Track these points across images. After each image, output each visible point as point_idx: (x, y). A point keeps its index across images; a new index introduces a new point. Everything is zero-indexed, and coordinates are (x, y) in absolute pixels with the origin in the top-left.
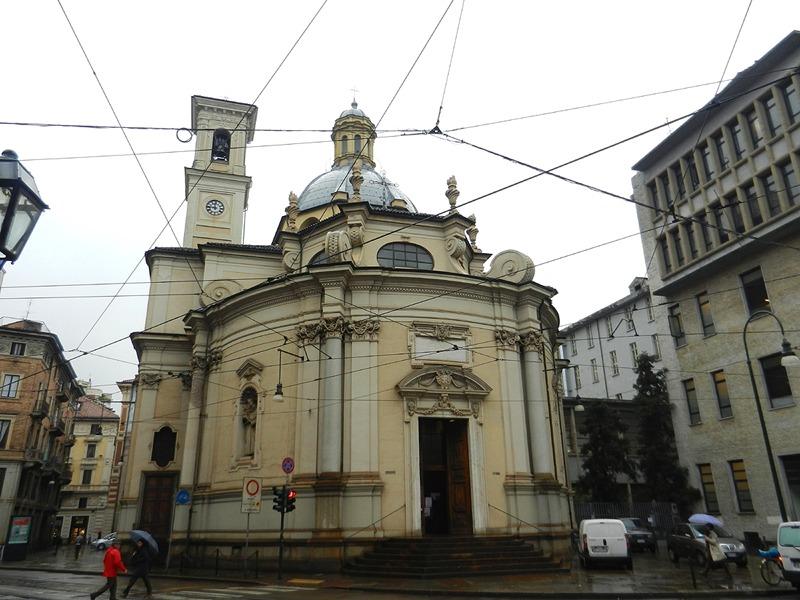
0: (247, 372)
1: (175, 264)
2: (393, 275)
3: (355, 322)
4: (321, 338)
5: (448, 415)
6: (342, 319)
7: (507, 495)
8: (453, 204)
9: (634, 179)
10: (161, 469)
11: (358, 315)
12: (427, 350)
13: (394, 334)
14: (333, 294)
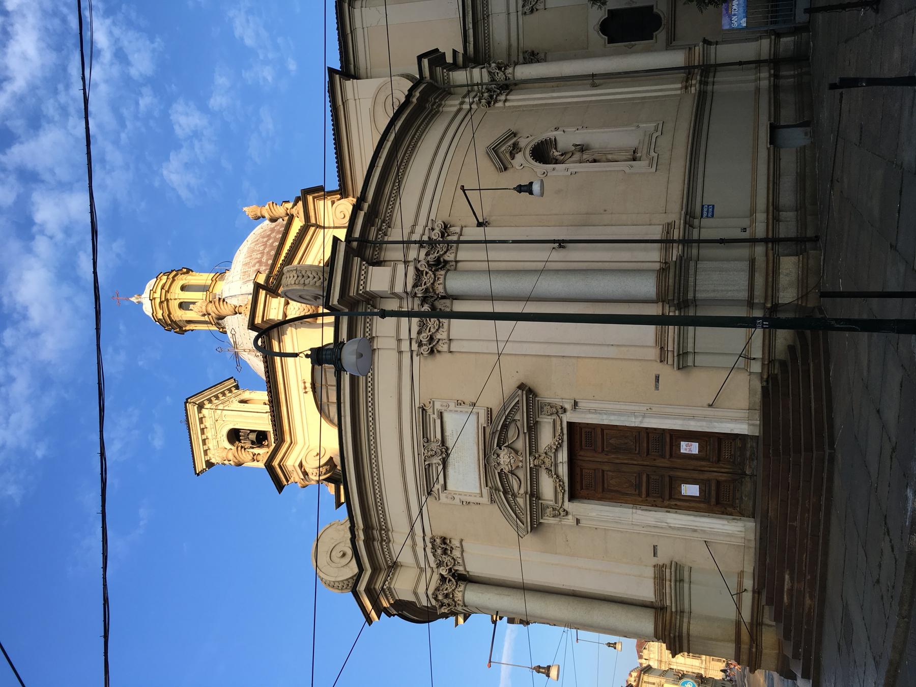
5: (563, 456)
12: (465, 474)
13: (442, 518)
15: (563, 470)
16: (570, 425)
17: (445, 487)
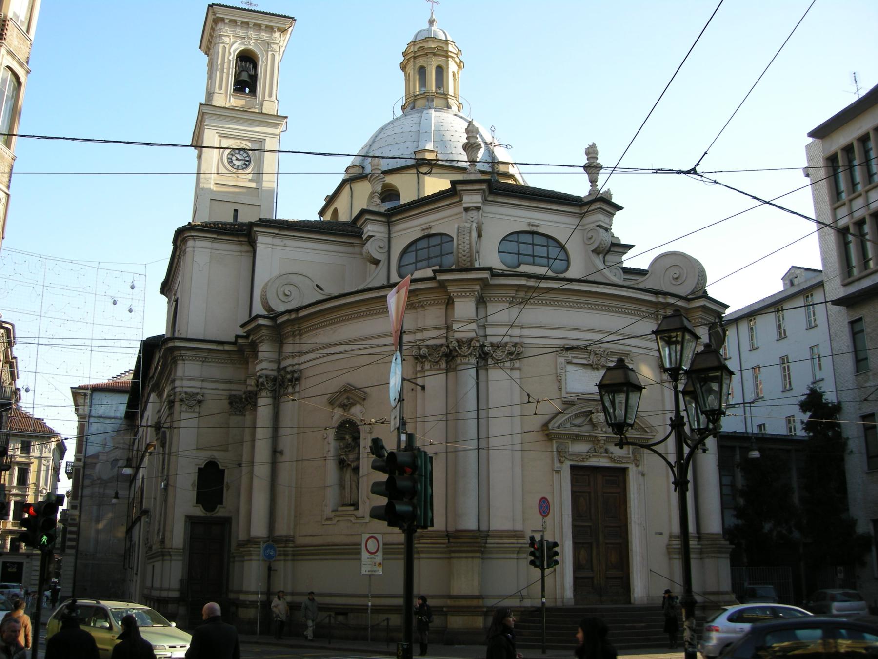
0: (343, 399)
1: (217, 245)
2: (541, 285)
3: (492, 345)
4: (447, 362)
5: (604, 462)
6: (478, 341)
7: (670, 559)
8: (593, 182)
9: (808, 147)
10: (209, 514)
11: (496, 334)
14: (464, 308)
15: (594, 462)
16: (624, 471)
17: (569, 363)
